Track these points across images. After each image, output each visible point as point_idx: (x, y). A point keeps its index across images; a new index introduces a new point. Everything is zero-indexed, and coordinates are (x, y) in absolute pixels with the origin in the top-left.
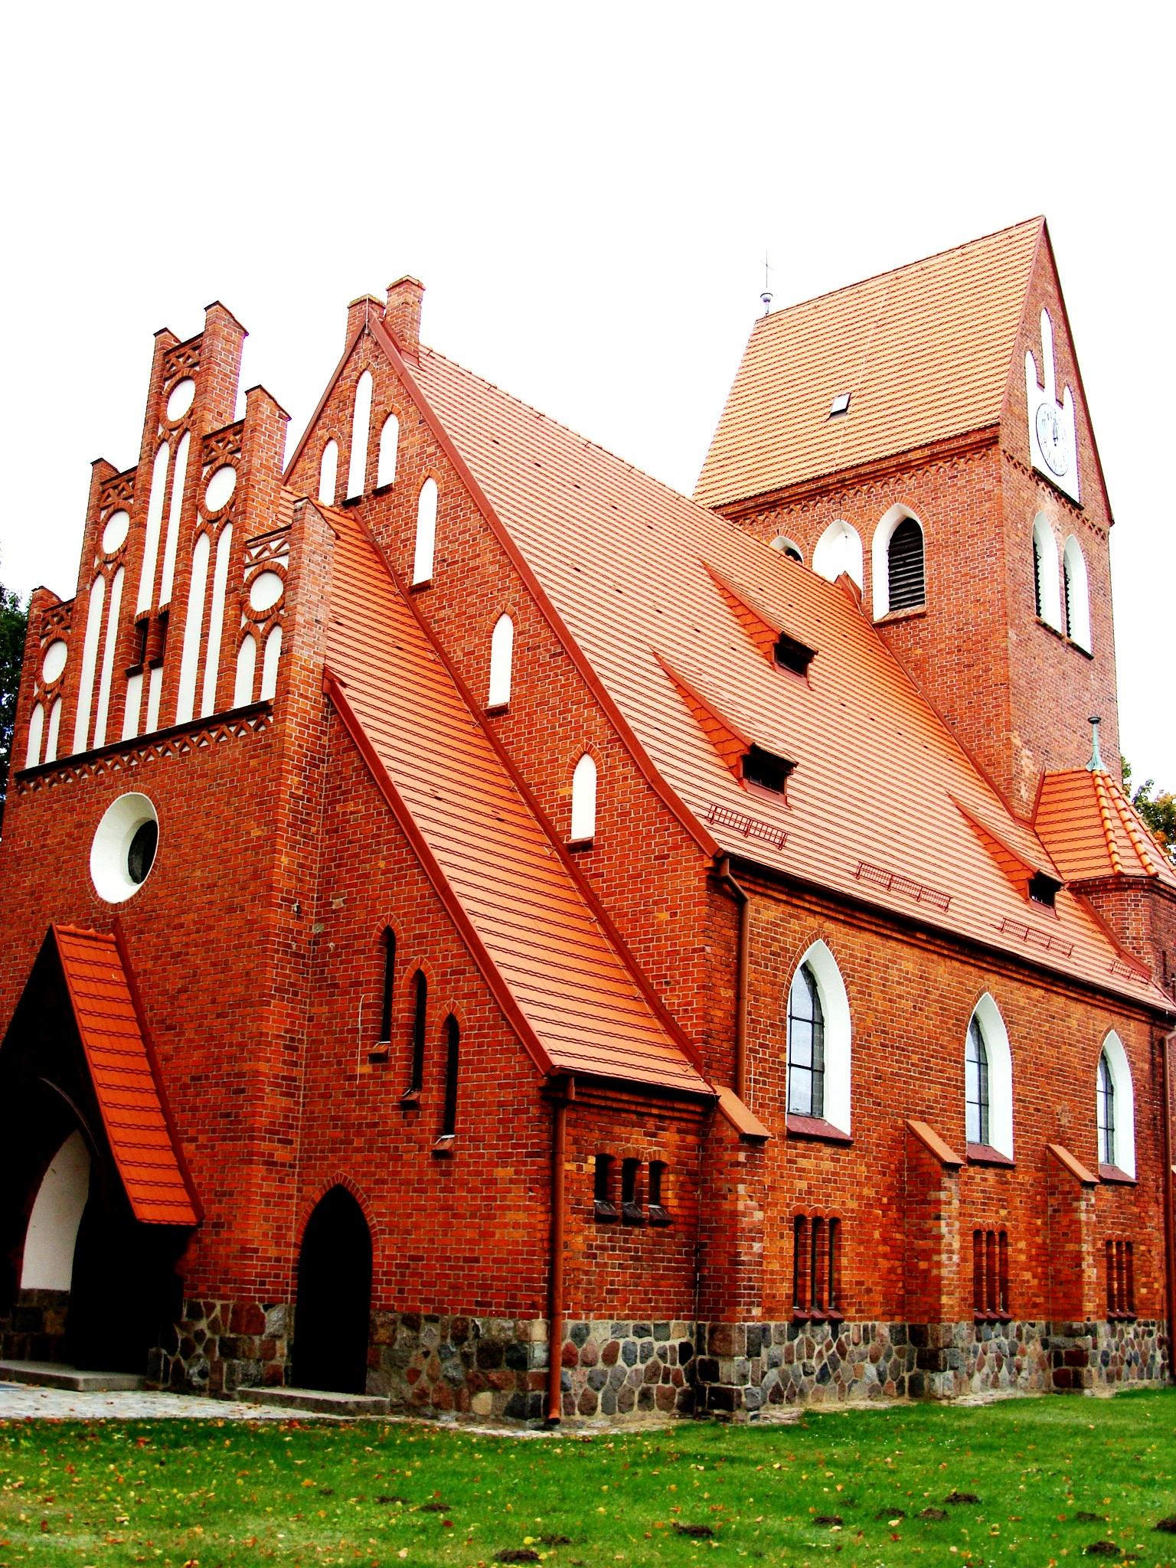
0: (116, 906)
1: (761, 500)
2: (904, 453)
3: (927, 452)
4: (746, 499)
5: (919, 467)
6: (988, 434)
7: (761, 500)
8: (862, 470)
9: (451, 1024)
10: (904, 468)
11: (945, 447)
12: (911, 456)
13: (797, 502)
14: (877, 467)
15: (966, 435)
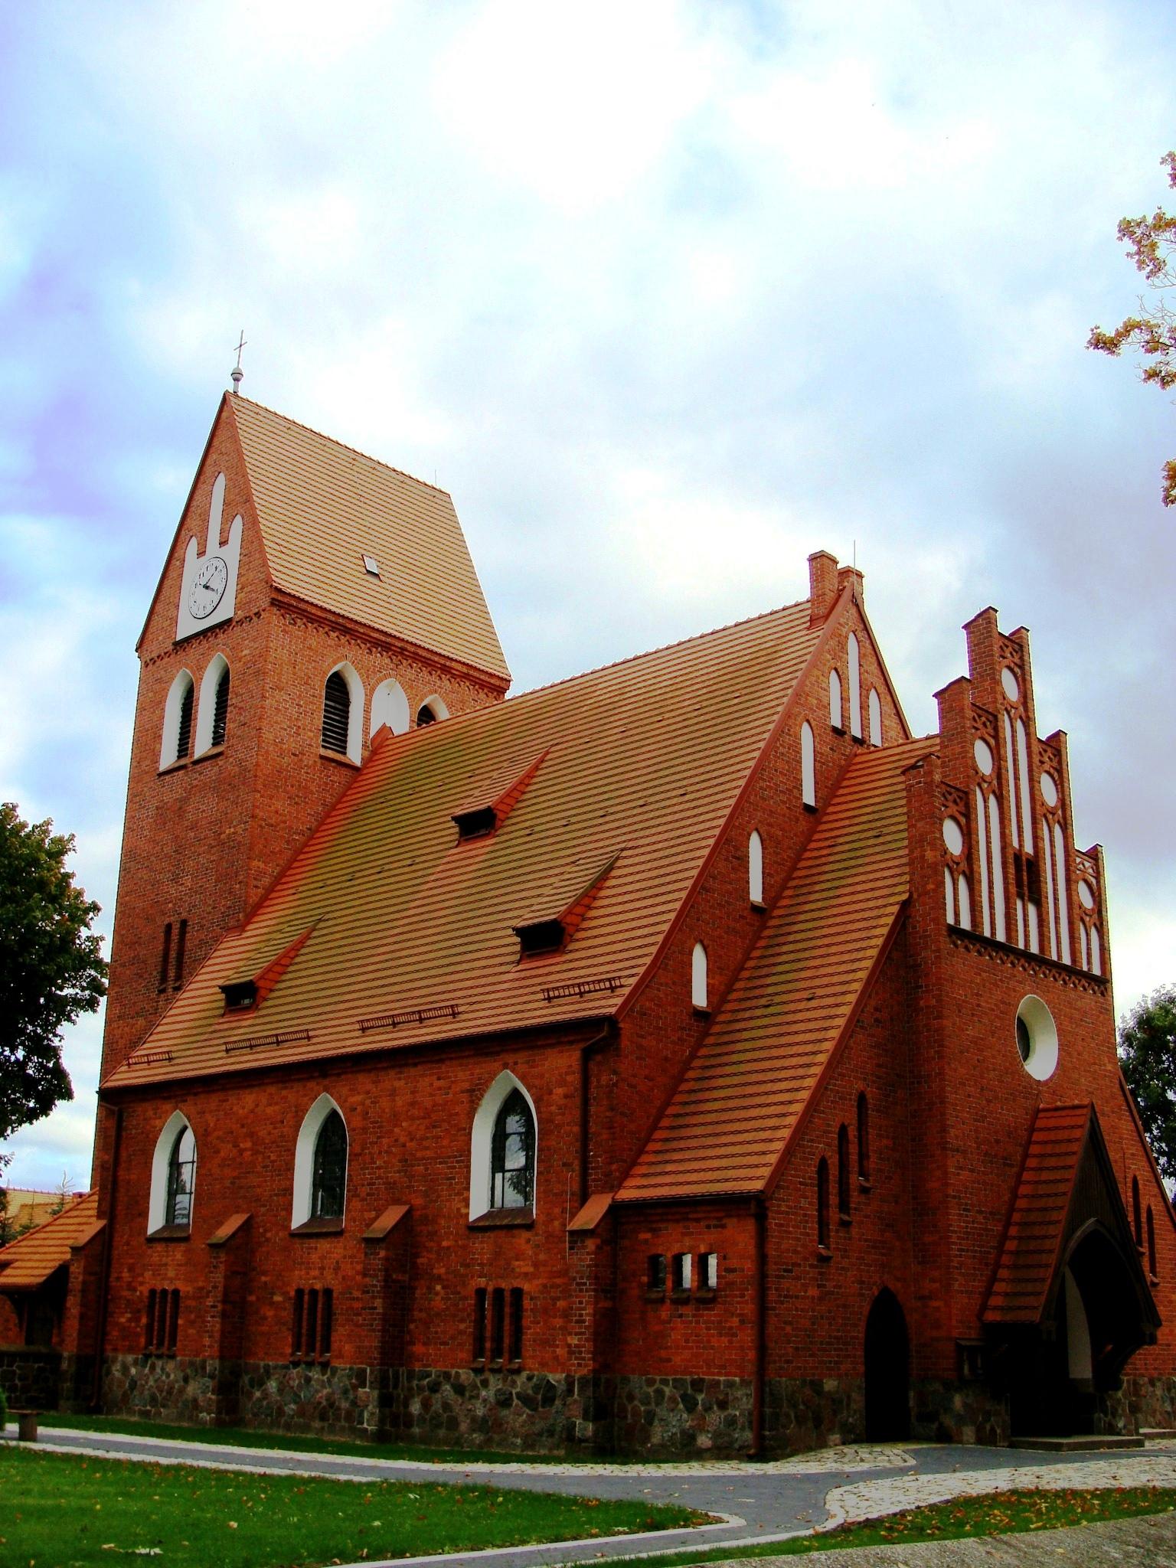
0: (1046, 1082)
1: (341, 620)
2: (452, 659)
3: (465, 670)
4: (330, 611)
5: (454, 676)
6: (498, 683)
7: (341, 620)
8: (420, 652)
9: (1149, 1210)
10: (446, 670)
11: (476, 674)
12: (454, 664)
13: (365, 641)
14: (429, 656)
15: (491, 675)
